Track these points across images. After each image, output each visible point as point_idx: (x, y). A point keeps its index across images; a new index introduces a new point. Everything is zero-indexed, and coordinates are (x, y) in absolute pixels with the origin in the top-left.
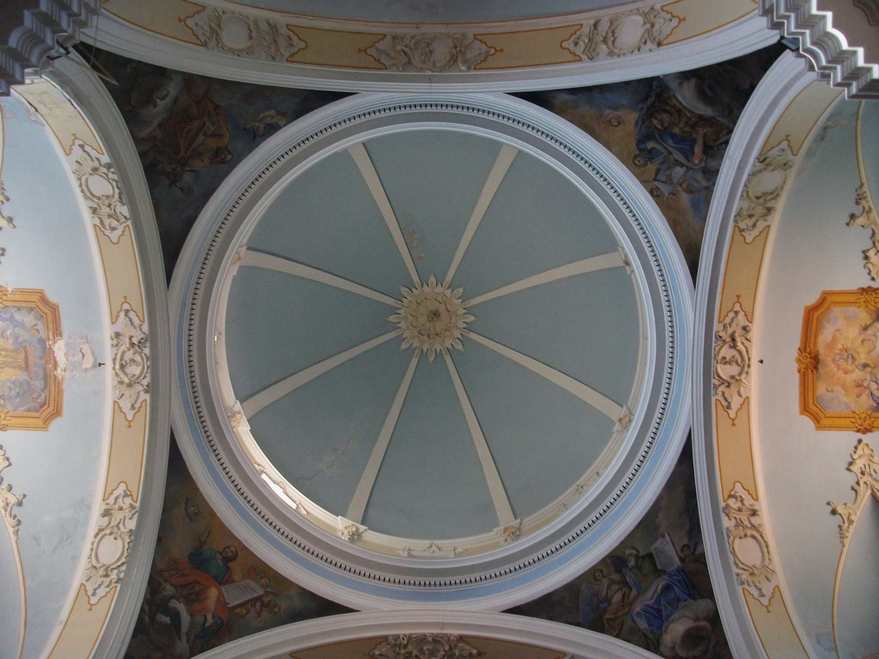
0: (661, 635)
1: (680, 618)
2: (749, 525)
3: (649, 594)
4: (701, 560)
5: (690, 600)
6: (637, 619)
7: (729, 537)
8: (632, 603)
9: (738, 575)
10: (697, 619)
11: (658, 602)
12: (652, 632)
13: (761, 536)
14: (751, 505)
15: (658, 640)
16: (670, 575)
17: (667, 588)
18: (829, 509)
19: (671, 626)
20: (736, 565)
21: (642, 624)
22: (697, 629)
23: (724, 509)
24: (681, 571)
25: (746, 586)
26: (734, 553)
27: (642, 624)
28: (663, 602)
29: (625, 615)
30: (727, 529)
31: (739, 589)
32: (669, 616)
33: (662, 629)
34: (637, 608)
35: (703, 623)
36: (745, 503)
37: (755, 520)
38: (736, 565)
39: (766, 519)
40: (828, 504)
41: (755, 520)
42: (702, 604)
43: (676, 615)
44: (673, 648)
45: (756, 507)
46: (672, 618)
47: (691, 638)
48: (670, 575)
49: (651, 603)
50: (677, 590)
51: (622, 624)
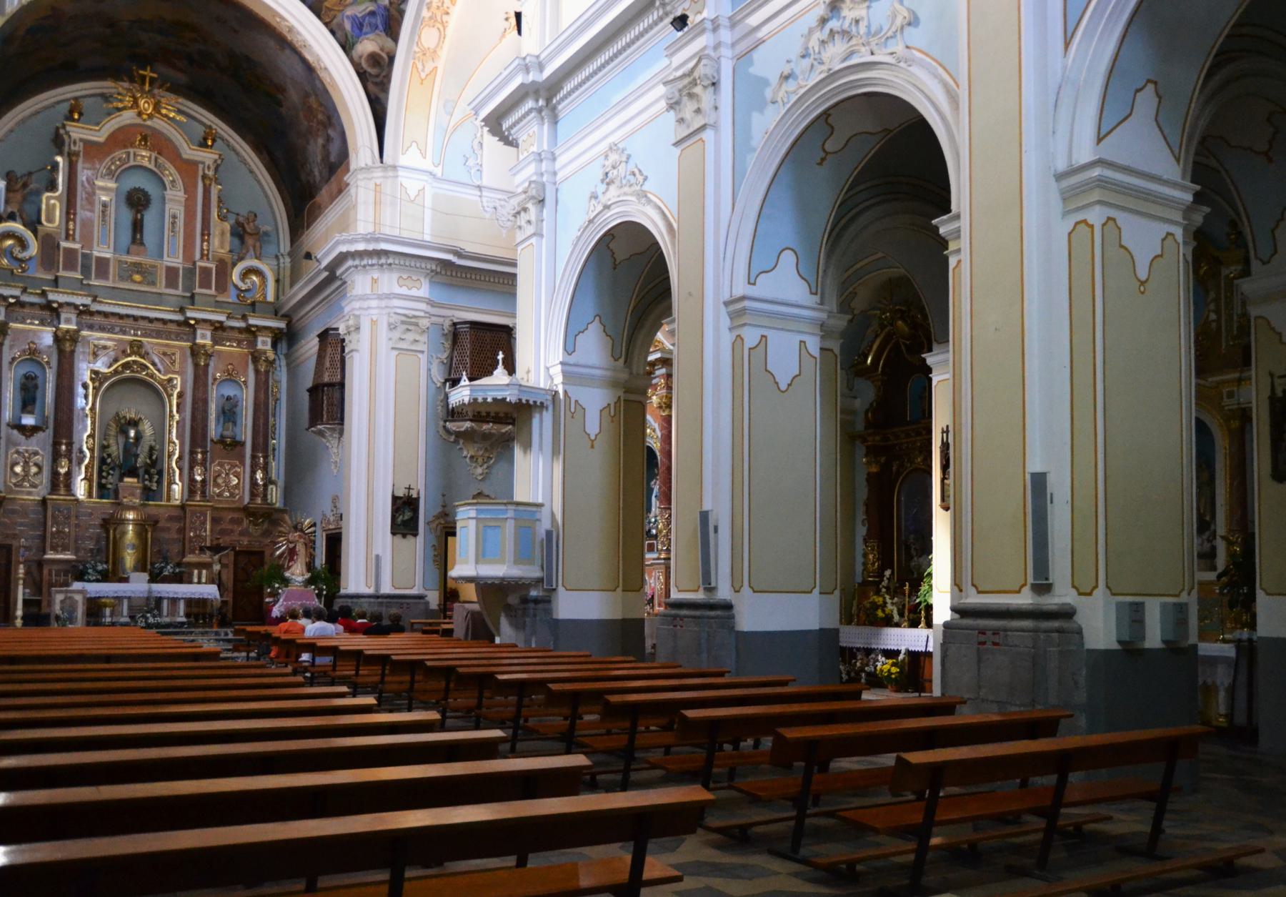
0: (357, 42)
1: (373, 40)
2: (439, 20)
3: (362, 8)
4: (402, 13)
5: (383, 34)
6: (346, 21)
7: (422, 24)
8: (346, 6)
9: (415, 52)
10: (382, 49)
11: (364, 17)
12: (352, 37)
13: (444, 29)
14: (448, 8)
15: (354, 44)
16: (379, 7)
17: (372, 13)
18: (506, 16)
19: (366, 41)
20: (417, 43)
21: (348, 26)
22: (380, 56)
23: (428, 4)
24: (385, 8)
25: (417, 62)
26: (420, 37)
27: (348, 26)
28: (366, 21)
29: (339, 11)
30: (424, 18)
31: (411, 62)
32: (366, 34)
33: (358, 38)
34: (349, 12)
35: (384, 56)
36: (445, 6)
37: (444, 18)
38: (417, 43)
39: (453, 21)
40: (507, 13)
41: (444, 18)
42: (389, 43)
43: (371, 36)
44: (361, 57)
45: (449, 11)
46: (367, 36)
47: (374, 59)
48: (379, 7)
49: (359, 15)
50: (379, 22)
51: (335, 17)
